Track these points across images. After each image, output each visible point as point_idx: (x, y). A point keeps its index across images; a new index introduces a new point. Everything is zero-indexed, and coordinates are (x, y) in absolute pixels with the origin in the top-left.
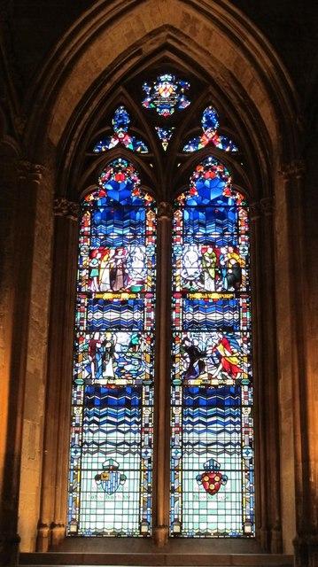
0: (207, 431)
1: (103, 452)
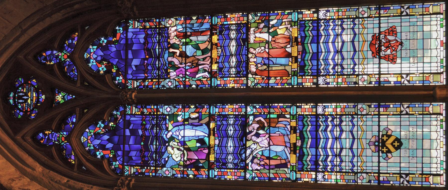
0: (341, 52)
1: (362, 152)
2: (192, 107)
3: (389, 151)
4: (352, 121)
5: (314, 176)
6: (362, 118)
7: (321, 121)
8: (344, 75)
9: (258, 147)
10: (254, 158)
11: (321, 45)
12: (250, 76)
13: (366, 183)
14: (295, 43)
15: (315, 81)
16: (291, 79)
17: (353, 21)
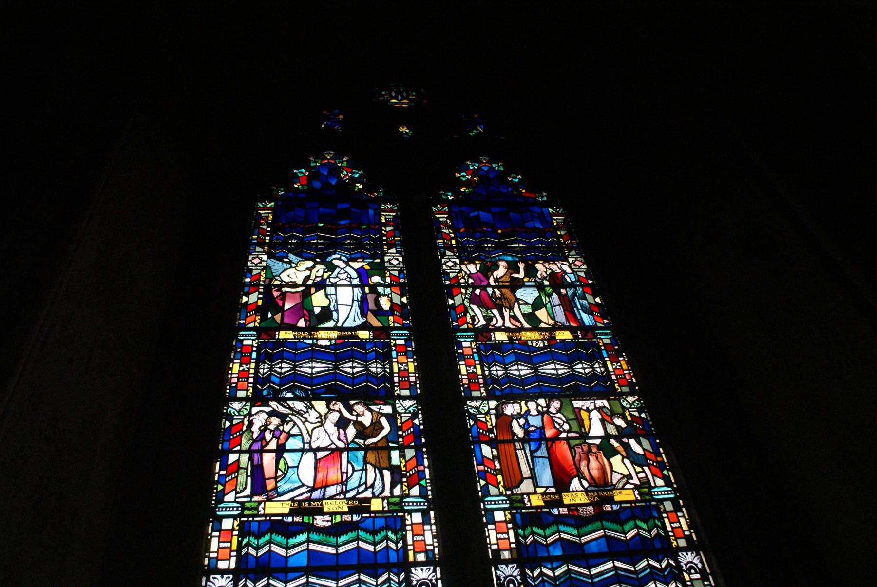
2: (404, 300)
5: (222, 565)
7: (389, 579)
9: (310, 427)
10: (283, 418)
11: (609, 565)
12: (493, 404)
14: (597, 498)
16: (501, 494)
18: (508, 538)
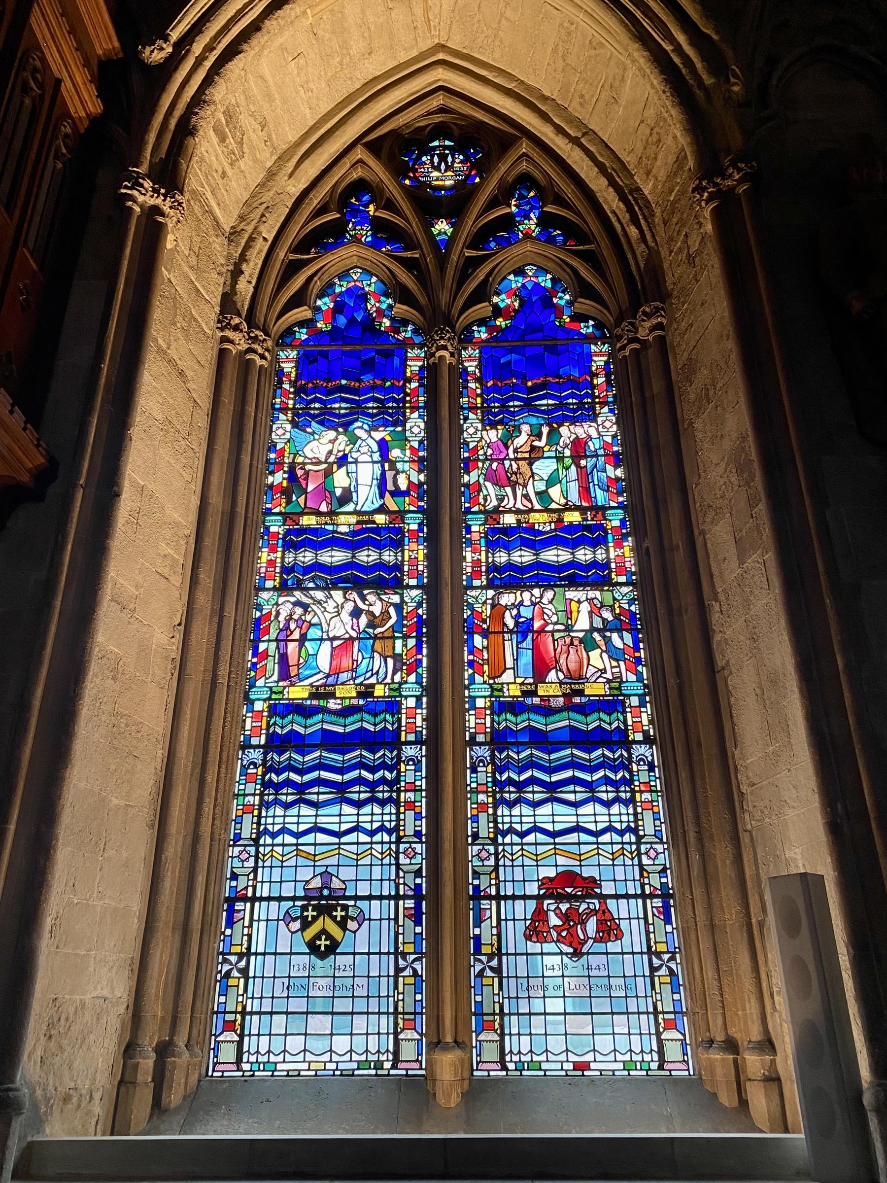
2: (422, 477)
3: (306, 924)
4: (382, 828)
5: (254, 741)
6: (390, 854)
7: (384, 755)
8: (495, 808)
9: (328, 616)
10: (305, 607)
11: (568, 752)
12: (491, 593)
13: (232, 868)
14: (569, 691)
15: (480, 738)
16: (485, 683)
17: (629, 829)
18: (485, 724)
